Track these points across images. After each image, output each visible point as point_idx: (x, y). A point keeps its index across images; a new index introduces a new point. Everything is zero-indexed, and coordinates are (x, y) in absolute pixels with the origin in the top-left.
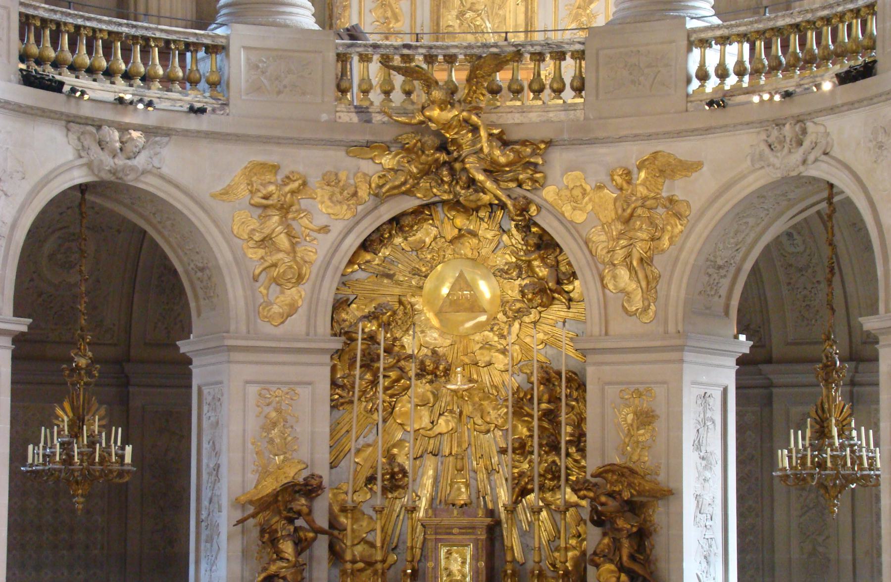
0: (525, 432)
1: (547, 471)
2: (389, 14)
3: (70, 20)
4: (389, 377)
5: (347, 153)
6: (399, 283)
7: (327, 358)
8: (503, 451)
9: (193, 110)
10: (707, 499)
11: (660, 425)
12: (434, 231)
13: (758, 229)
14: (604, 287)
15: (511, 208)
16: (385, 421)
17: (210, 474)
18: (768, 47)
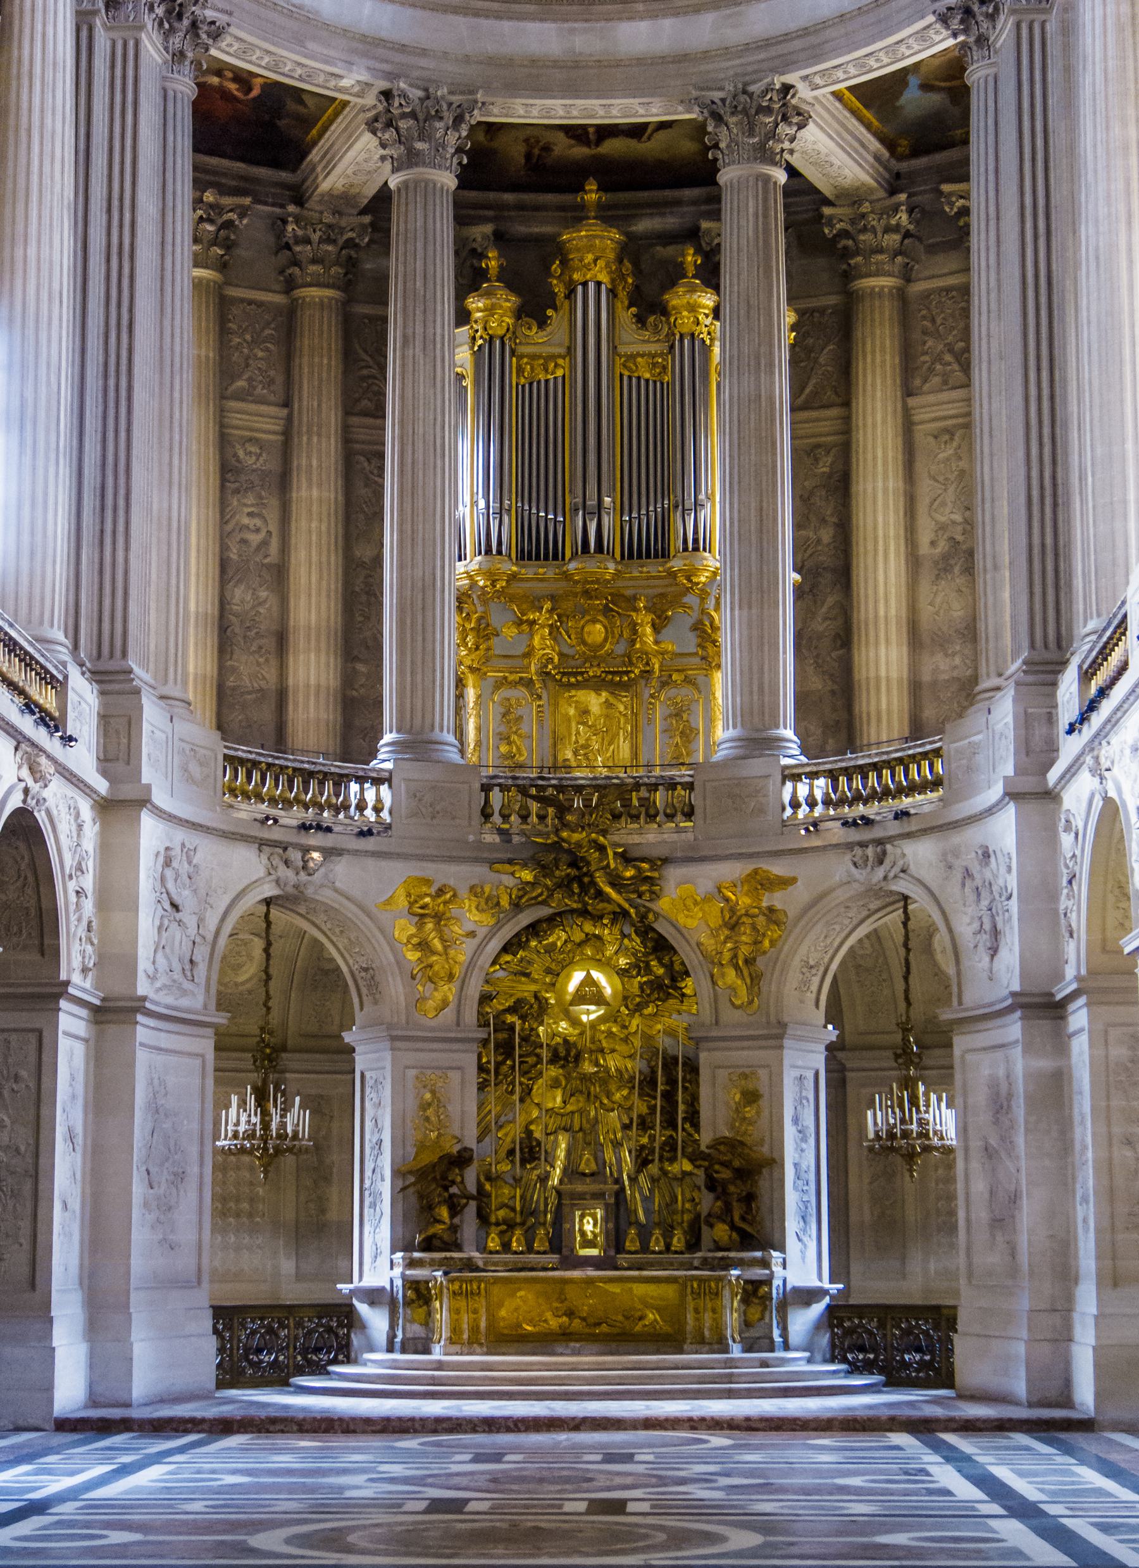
0: (645, 1110)
1: (665, 1144)
6: (535, 981)
7: (474, 1046)
8: (626, 1127)
9: (362, 834)
10: (804, 1167)
11: (764, 1103)
12: (564, 936)
13: (843, 935)
14: (714, 983)
16: (522, 1100)
17: (373, 1148)
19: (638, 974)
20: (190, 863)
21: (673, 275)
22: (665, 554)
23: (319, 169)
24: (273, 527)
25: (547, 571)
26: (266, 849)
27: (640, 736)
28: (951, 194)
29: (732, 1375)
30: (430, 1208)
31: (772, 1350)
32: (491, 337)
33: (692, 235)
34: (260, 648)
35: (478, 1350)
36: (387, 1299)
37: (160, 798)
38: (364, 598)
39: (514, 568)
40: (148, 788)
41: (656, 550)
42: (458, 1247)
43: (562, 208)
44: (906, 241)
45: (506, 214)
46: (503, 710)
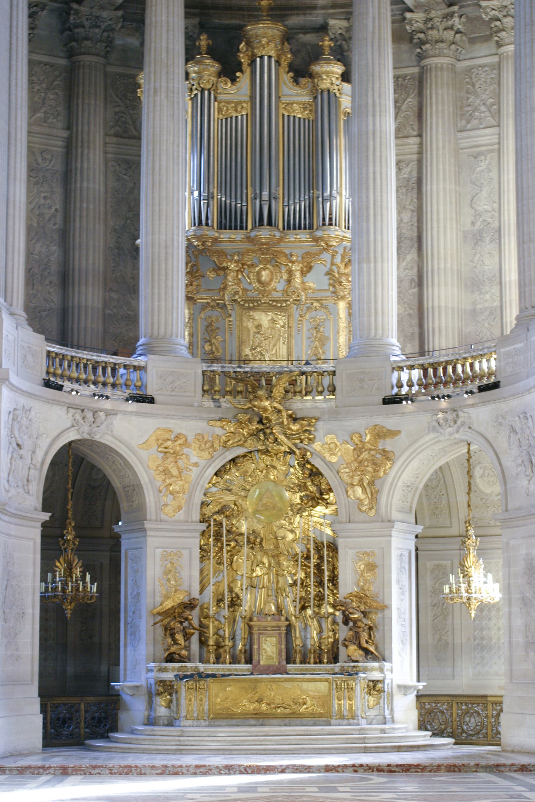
2: (214, 349)
3: (69, 353)
4: (230, 545)
5: (208, 424)
6: (235, 494)
15: (298, 454)
18: (435, 370)
19: (300, 490)
20: (27, 418)
21: (316, 55)
22: (311, 227)
26: (71, 410)
27: (293, 342)
28: (487, 7)
29: (365, 738)
30: (172, 635)
31: (385, 723)
33: (323, 28)
35: (203, 724)
36: (144, 691)
37: (13, 379)
39: (217, 235)
40: (7, 370)
41: (305, 224)
42: (188, 659)
44: (457, 35)
46: (207, 324)
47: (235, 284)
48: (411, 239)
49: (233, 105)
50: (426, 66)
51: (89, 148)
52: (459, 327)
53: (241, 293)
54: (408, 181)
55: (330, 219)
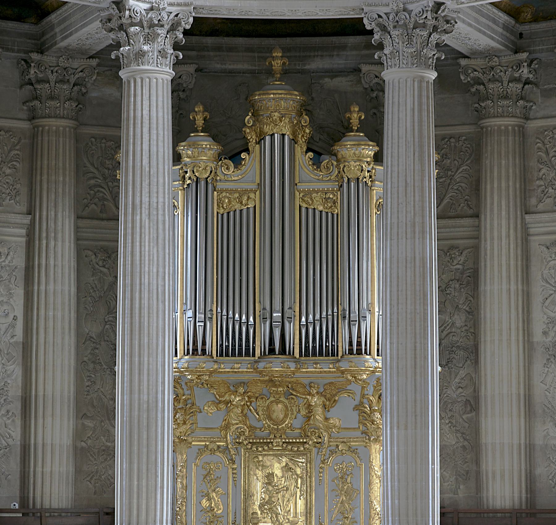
23: (57, 30)
24: (19, 312)
25: (240, 366)
32: (197, 178)
34: (8, 412)
38: (91, 366)
43: (250, 49)
44: (526, 86)
45: (206, 53)
47: (240, 422)
48: (465, 349)
49: (237, 195)
50: (487, 127)
51: (55, 239)
52: (526, 470)
53: (247, 434)
54: (462, 273)
55: (359, 344)
